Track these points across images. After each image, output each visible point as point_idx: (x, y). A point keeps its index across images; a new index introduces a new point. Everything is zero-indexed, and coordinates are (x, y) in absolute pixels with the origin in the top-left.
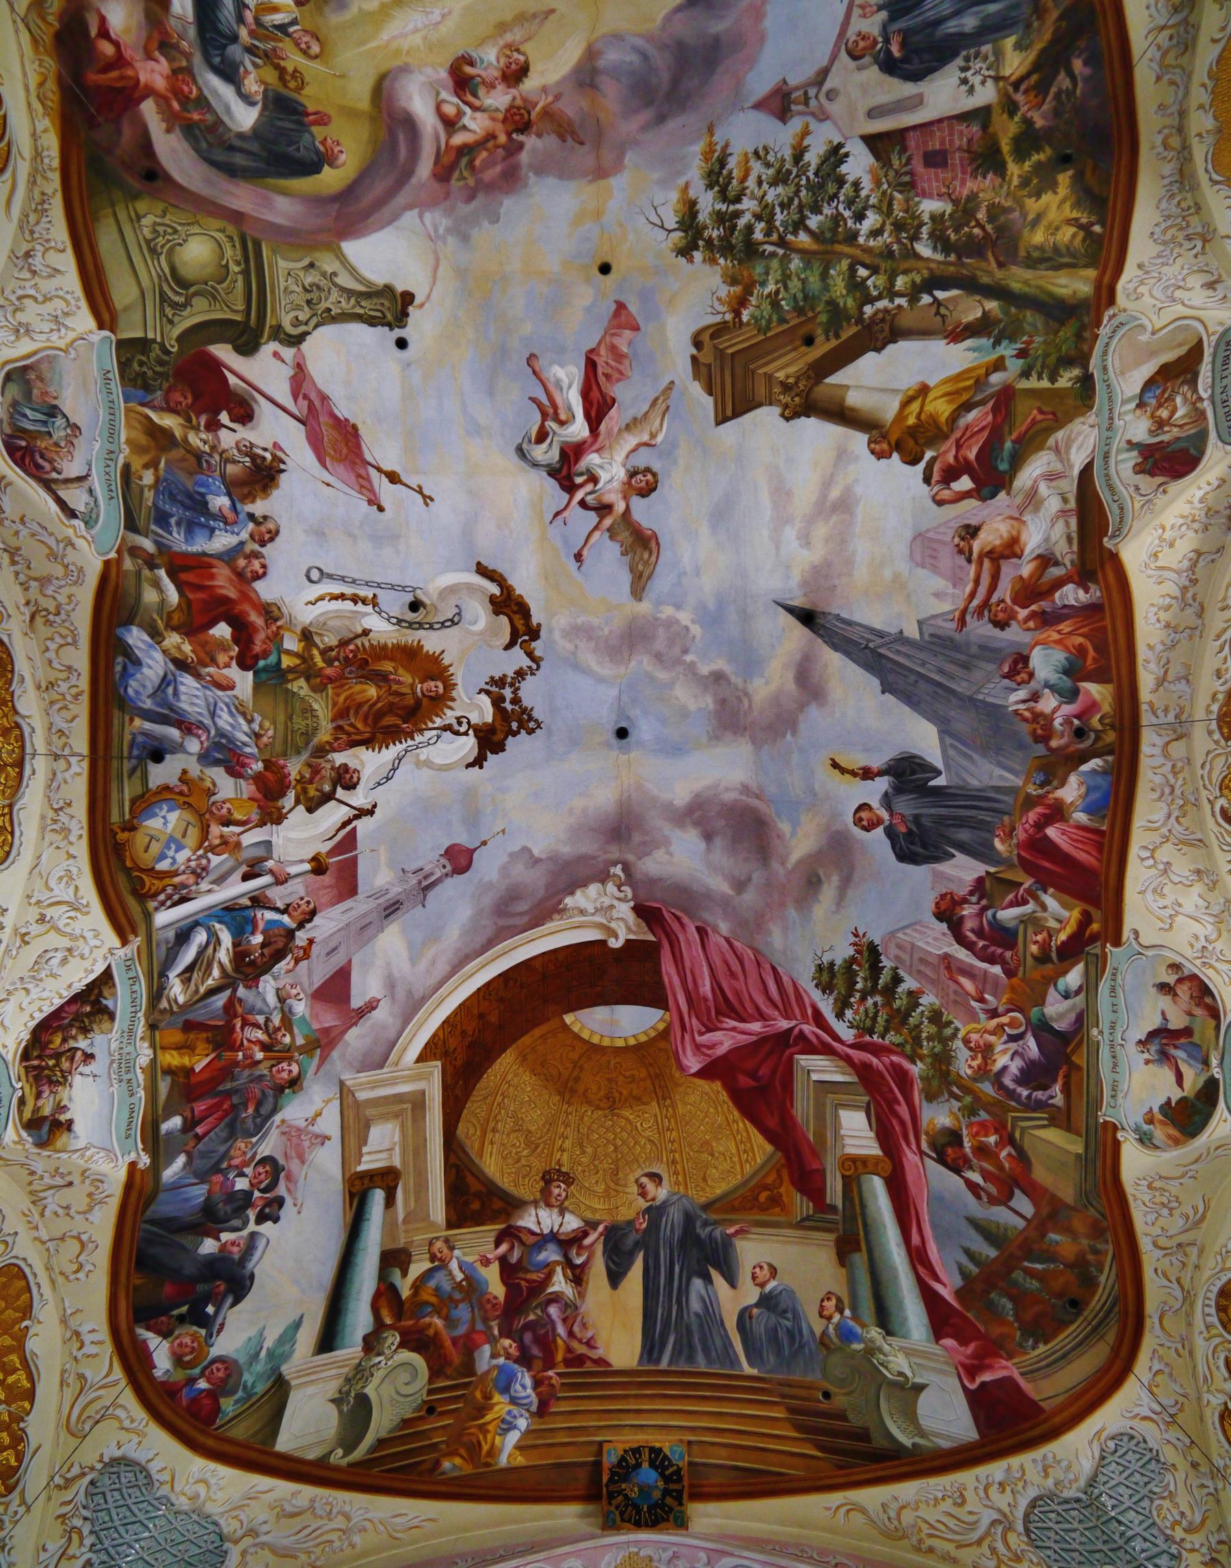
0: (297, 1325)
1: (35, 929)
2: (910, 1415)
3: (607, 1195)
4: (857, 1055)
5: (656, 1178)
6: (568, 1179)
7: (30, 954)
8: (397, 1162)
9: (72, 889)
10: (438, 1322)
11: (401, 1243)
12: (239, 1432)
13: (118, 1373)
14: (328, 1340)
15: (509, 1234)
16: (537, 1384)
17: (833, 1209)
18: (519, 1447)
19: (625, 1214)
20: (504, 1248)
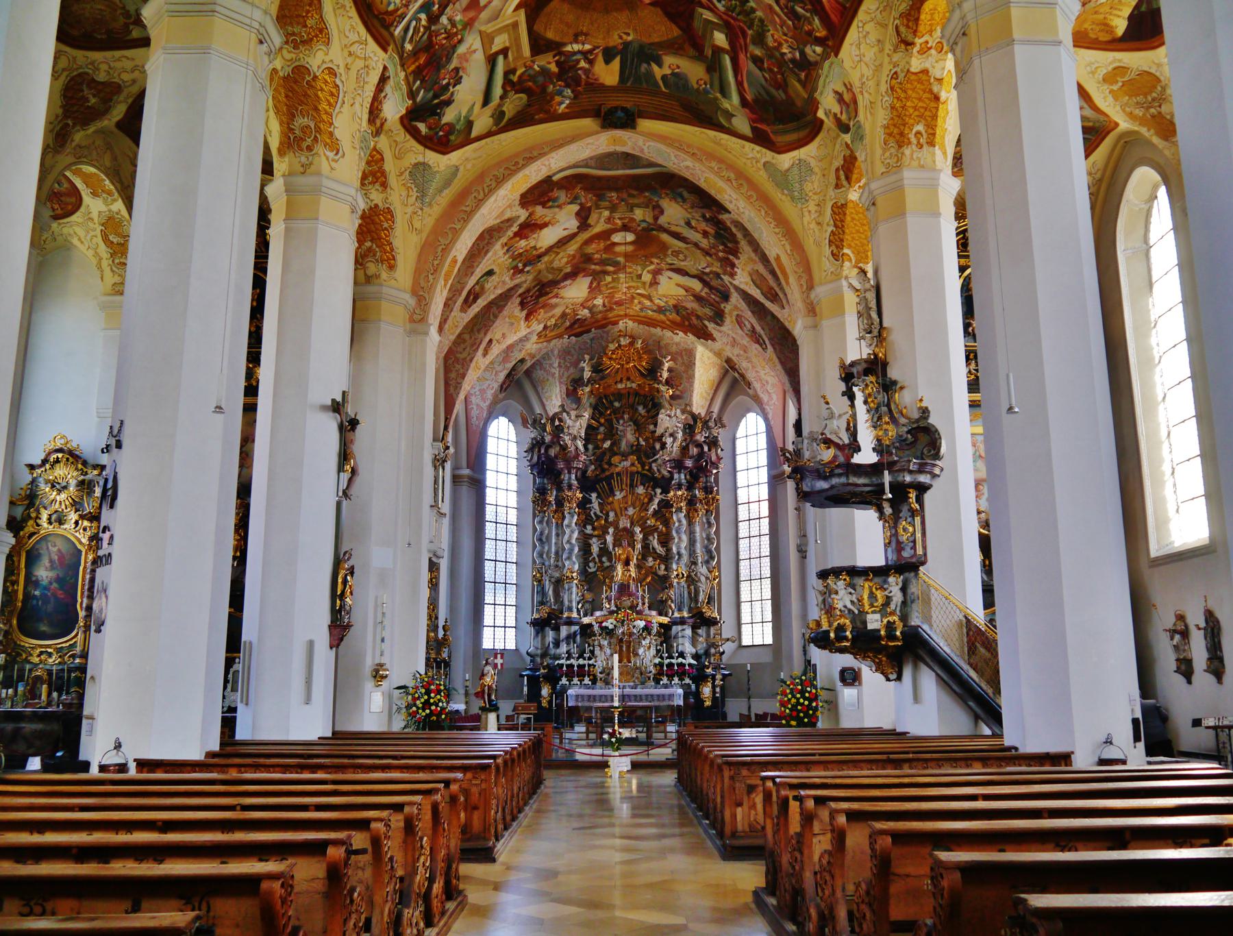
0: (474, 105)
1: (349, 60)
2: (729, 121)
3: (604, 39)
4: (724, 17)
5: (628, 34)
6: (586, 35)
7: (353, 73)
8: (507, 44)
9: (356, 35)
10: (530, 84)
11: (512, 66)
12: (458, 141)
13: (408, 137)
14: (486, 101)
15: (561, 53)
16: (572, 92)
17: (707, 57)
18: (566, 108)
19: (611, 44)
20: (557, 58)
